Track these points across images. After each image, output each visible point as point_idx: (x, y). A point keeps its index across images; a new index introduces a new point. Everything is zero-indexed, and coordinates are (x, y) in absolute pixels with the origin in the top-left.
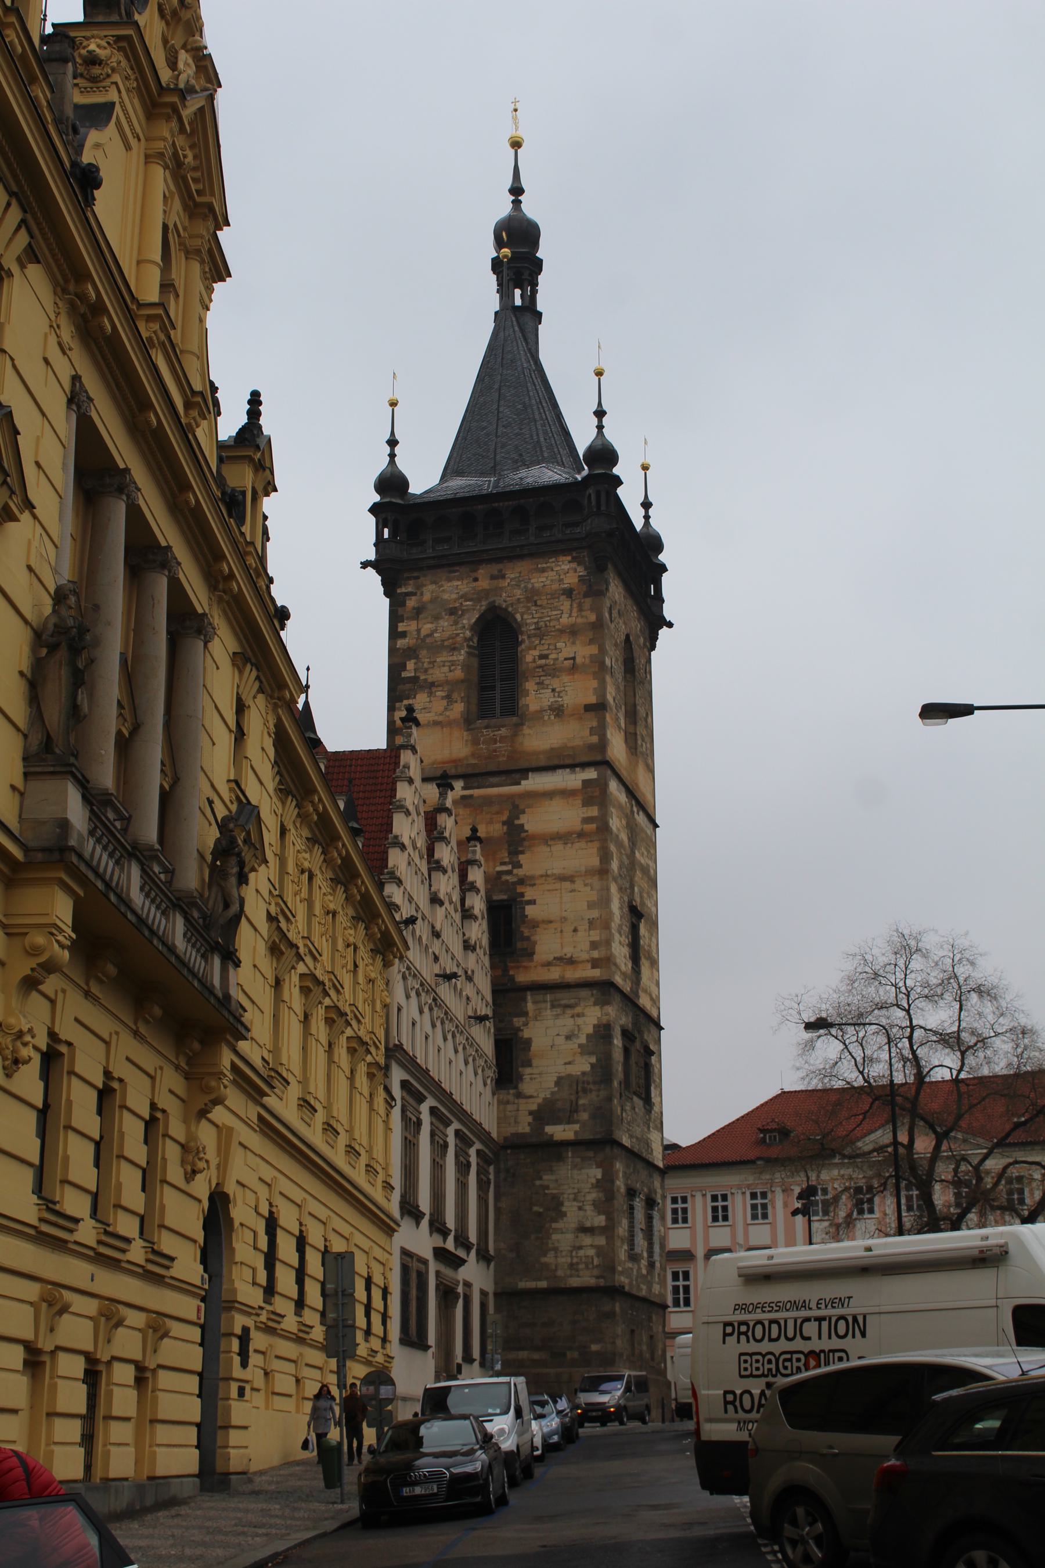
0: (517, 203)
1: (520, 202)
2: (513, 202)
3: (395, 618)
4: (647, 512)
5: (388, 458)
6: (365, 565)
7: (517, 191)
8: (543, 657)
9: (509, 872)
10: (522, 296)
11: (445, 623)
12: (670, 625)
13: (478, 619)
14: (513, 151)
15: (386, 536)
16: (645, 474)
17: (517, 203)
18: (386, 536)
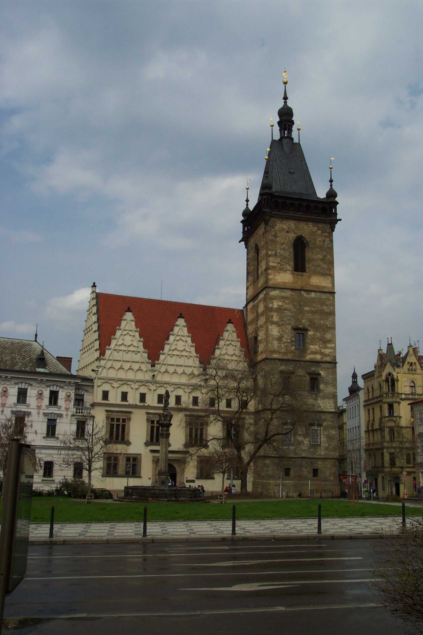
0: (285, 102)
1: (287, 102)
2: (284, 102)
3: (248, 254)
4: (331, 183)
5: (246, 206)
6: (240, 242)
7: (285, 98)
8: (260, 257)
9: (257, 327)
10: (285, 133)
11: (251, 253)
12: (340, 220)
13: (255, 249)
14: (284, 85)
15: (246, 230)
16: (331, 170)
17: (285, 102)
18: (246, 230)
